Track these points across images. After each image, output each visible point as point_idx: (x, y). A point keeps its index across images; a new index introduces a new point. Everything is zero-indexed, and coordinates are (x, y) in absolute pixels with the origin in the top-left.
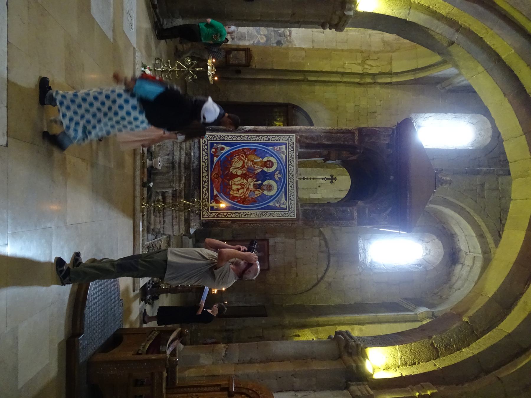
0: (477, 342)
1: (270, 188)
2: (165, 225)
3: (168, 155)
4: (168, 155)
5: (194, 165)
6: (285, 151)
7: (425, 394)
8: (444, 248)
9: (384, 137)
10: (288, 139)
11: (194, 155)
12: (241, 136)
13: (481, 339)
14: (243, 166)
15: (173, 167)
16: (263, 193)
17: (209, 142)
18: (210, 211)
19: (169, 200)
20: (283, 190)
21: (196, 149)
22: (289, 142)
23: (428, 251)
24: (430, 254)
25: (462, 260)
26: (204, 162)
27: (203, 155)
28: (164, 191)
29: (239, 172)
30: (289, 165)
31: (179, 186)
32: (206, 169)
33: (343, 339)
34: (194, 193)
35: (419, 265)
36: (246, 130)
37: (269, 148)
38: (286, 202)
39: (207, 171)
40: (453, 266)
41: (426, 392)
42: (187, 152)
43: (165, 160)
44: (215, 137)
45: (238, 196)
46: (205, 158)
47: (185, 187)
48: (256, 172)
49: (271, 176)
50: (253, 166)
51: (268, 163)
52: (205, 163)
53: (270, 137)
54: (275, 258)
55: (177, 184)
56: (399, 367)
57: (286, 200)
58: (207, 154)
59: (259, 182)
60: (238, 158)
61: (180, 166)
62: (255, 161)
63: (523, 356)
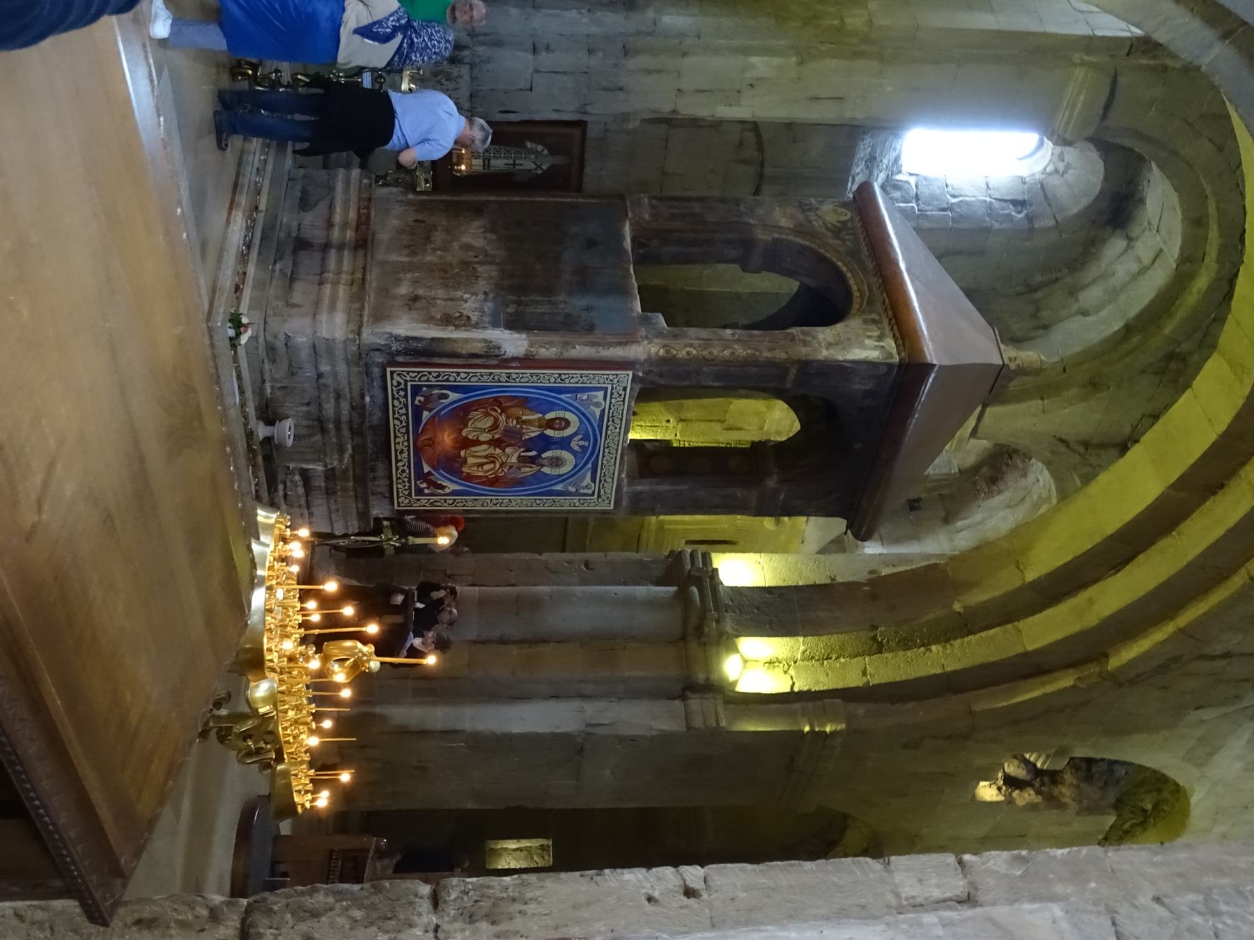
0: (966, 639)
1: (557, 462)
3: (308, 404)
4: (308, 404)
6: (603, 403)
7: (822, 729)
8: (1106, 179)
10: (611, 381)
12: (491, 373)
13: (978, 636)
14: (495, 426)
15: (323, 430)
16: (539, 470)
17: (409, 384)
18: (413, 496)
19: (320, 482)
20: (590, 465)
21: (378, 392)
22: (614, 386)
23: (1065, 164)
24: (1066, 176)
25: (1135, 230)
26: (398, 419)
27: (393, 406)
28: (305, 466)
29: (484, 437)
30: (608, 426)
31: (341, 461)
32: (403, 430)
33: (698, 603)
35: (1018, 204)
36: (505, 357)
37: (563, 396)
38: (593, 485)
39: (405, 434)
40: (1109, 230)
41: (824, 725)
42: (354, 404)
43: (301, 414)
44: (425, 375)
45: (481, 474)
46: (398, 413)
47: (353, 463)
48: (527, 437)
49: (564, 444)
50: (518, 426)
51: (558, 421)
52: (401, 422)
53: (567, 376)
54: (601, 170)
56: (795, 662)
57: (594, 480)
58: (406, 406)
59: (533, 453)
60: (483, 412)
61: (338, 428)
62: (524, 418)
63: (1036, 680)
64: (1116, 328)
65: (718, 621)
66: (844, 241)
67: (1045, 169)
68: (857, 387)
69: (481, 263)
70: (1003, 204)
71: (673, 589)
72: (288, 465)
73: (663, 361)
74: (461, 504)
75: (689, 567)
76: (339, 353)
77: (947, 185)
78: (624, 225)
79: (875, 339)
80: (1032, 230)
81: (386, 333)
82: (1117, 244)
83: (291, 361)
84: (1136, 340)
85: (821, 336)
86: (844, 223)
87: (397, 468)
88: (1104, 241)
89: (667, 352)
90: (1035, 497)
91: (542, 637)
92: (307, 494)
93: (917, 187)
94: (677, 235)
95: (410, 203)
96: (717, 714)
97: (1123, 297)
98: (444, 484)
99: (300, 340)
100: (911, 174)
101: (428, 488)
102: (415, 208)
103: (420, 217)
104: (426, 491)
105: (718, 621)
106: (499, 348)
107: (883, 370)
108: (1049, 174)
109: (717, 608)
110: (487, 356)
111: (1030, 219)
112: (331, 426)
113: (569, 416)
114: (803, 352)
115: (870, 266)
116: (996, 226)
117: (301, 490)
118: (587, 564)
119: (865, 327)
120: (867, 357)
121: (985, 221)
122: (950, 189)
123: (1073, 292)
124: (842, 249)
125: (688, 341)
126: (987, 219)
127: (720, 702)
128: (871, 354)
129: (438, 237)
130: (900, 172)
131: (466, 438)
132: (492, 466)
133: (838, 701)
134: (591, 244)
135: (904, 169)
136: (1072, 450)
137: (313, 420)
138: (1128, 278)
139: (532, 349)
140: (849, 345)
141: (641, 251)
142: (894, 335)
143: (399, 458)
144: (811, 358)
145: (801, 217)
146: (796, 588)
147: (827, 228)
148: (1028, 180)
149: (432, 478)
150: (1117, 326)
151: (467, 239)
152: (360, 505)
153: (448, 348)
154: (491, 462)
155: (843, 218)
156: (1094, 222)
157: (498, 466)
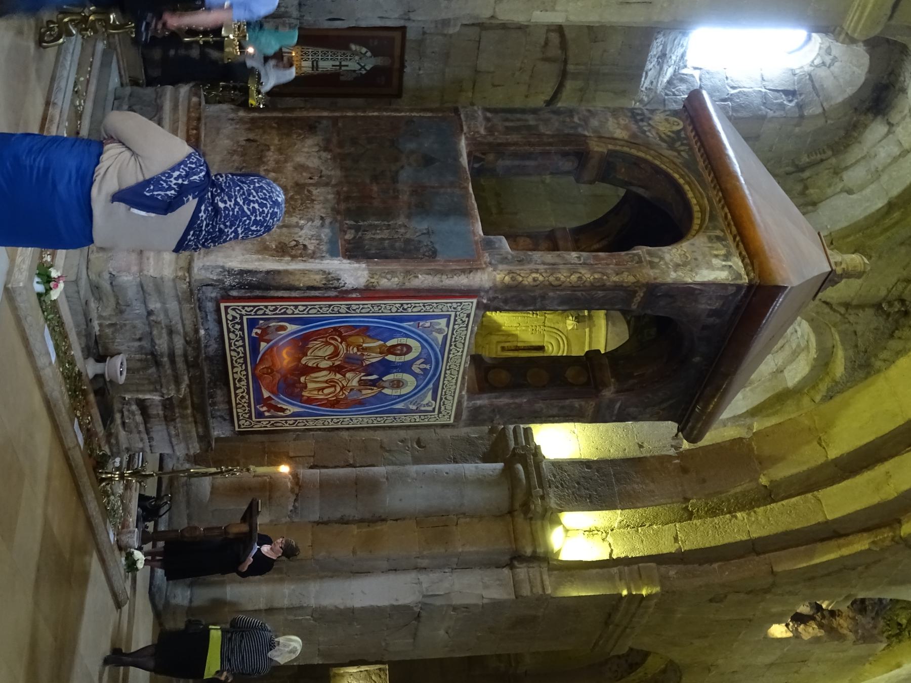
0: (768, 506)
1: (398, 384)
2: (154, 443)
3: (140, 339)
4: (140, 339)
5: (210, 349)
6: (446, 329)
7: (638, 593)
8: (870, 71)
9: (710, 299)
10: (454, 308)
11: (208, 334)
12: (330, 306)
13: (780, 503)
14: (335, 354)
15: (158, 364)
16: (380, 392)
17: (245, 318)
20: (431, 386)
21: (212, 325)
22: (458, 313)
23: (831, 57)
24: (832, 68)
25: (895, 117)
26: (234, 350)
27: (229, 339)
28: (141, 396)
29: (324, 364)
30: (450, 350)
31: (178, 390)
32: (241, 361)
33: (524, 481)
34: (215, 392)
35: (790, 93)
37: (404, 325)
38: (434, 402)
39: (243, 364)
40: (870, 116)
41: (640, 589)
43: (133, 349)
44: (262, 309)
46: (235, 345)
47: (191, 392)
48: (368, 363)
49: (406, 367)
50: (359, 353)
51: (399, 348)
52: (238, 353)
53: (409, 305)
54: (420, 69)
55: (172, 387)
56: (612, 530)
57: (434, 399)
58: (243, 339)
59: (375, 377)
60: (322, 342)
62: (364, 345)
63: (833, 543)
64: (880, 205)
65: (542, 498)
66: (679, 152)
67: (813, 62)
68: (703, 306)
69: (316, 185)
70: (777, 94)
71: (499, 466)
72: (123, 396)
73: (508, 288)
74: (303, 424)
75: (512, 444)
76: (168, 288)
77: (727, 78)
78: (460, 140)
79: (722, 258)
80: (802, 117)
81: (218, 267)
82: (877, 129)
83: (117, 299)
84: (896, 215)
85: (667, 257)
86: (678, 132)
87: (236, 395)
88: (866, 126)
89: (513, 279)
90: (794, 346)
91: (380, 517)
92: (146, 422)
93: (700, 79)
94: (512, 148)
95: (241, 121)
96: (542, 582)
97: (885, 178)
98: (285, 407)
99: (126, 278)
100: (695, 68)
101: (268, 411)
102: (247, 126)
103: (251, 136)
104: (267, 414)
105: (542, 498)
106: (338, 280)
107: (732, 290)
108: (816, 66)
109: (541, 485)
110: (326, 288)
111: (800, 106)
112: (165, 359)
113: (410, 342)
114: (650, 274)
115: (709, 179)
116: (771, 113)
117: (139, 418)
118: (419, 442)
119: (710, 245)
120: (716, 278)
121: (760, 110)
122: (729, 81)
123: (837, 172)
124: (678, 161)
125: (532, 266)
126: (763, 107)
127: (545, 570)
128: (722, 276)
129: (271, 156)
130: (685, 66)
131: (306, 366)
132: (332, 389)
133: (653, 565)
134: (428, 161)
135: (689, 64)
136: (834, 311)
137: (146, 354)
138: (889, 161)
139: (373, 280)
140: (697, 266)
141: (476, 166)
142: (740, 254)
143: (238, 385)
144: (659, 281)
145: (634, 127)
146: (612, 462)
147: (661, 139)
148: (797, 72)
149: (273, 402)
150: (880, 204)
151: (300, 159)
152: (200, 430)
153: (286, 280)
154: (332, 386)
155: (676, 128)
156: (856, 109)
157: (338, 389)
